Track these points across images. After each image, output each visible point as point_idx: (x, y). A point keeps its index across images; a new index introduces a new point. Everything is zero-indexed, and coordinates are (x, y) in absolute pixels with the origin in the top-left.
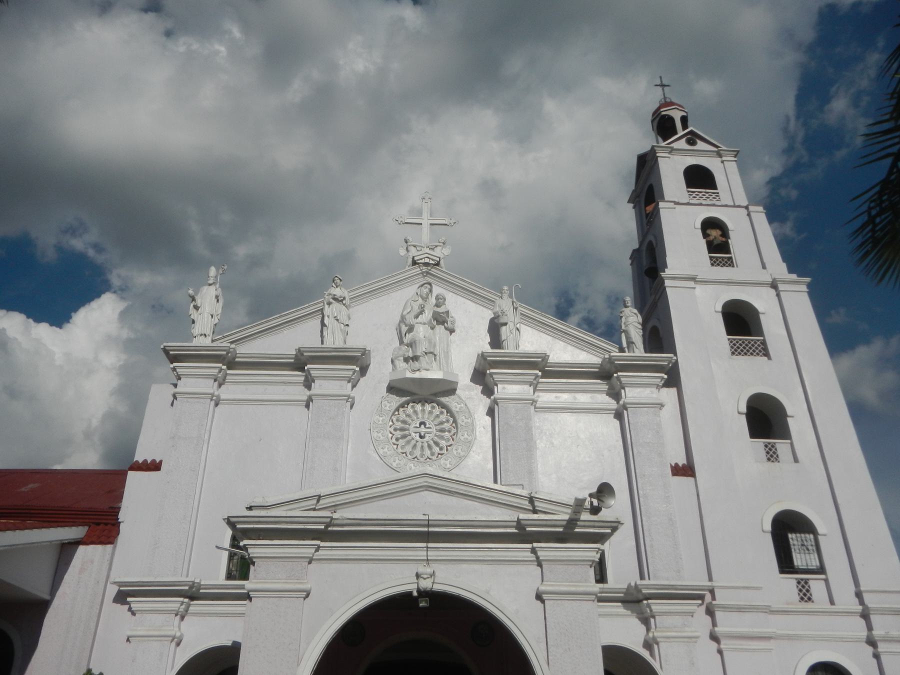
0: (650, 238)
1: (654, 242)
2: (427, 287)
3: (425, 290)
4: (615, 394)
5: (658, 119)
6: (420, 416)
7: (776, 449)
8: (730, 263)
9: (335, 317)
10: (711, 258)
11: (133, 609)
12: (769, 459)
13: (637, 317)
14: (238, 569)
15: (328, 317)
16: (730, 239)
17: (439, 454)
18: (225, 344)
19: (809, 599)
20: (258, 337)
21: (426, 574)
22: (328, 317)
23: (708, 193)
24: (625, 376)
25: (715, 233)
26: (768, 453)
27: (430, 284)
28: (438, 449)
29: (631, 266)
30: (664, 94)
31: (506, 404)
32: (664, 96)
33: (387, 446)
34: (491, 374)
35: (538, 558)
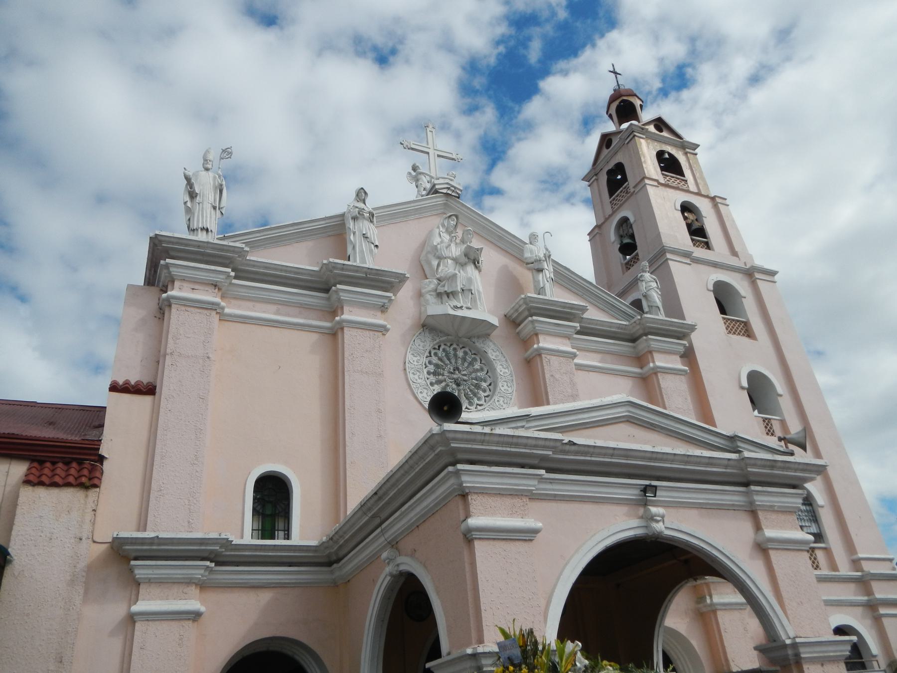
0: (625, 212)
1: (632, 220)
2: (454, 220)
3: (453, 223)
4: (640, 359)
5: (616, 103)
6: (453, 361)
7: (771, 425)
8: (708, 246)
9: (364, 234)
10: (693, 240)
11: (137, 577)
12: (767, 434)
13: (657, 283)
14: (260, 528)
15: (354, 233)
16: (704, 224)
17: (477, 405)
18: (238, 244)
19: (817, 566)
20: (261, 245)
21: (659, 516)
22: (354, 233)
23: (678, 179)
24: (654, 341)
25: (691, 217)
26: (766, 427)
27: (457, 217)
28: (476, 399)
29: (589, 242)
30: (617, 82)
31: (549, 356)
32: (618, 83)
33: (425, 391)
34: (532, 322)
35: (752, 503)
